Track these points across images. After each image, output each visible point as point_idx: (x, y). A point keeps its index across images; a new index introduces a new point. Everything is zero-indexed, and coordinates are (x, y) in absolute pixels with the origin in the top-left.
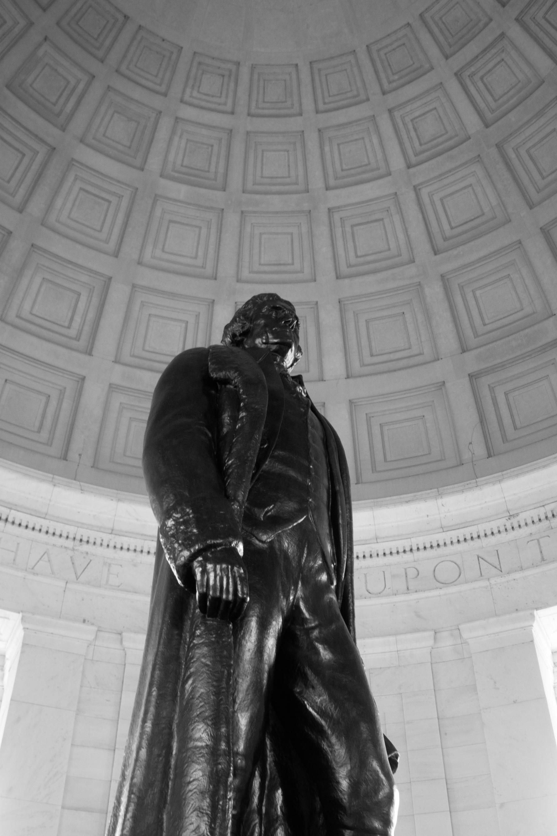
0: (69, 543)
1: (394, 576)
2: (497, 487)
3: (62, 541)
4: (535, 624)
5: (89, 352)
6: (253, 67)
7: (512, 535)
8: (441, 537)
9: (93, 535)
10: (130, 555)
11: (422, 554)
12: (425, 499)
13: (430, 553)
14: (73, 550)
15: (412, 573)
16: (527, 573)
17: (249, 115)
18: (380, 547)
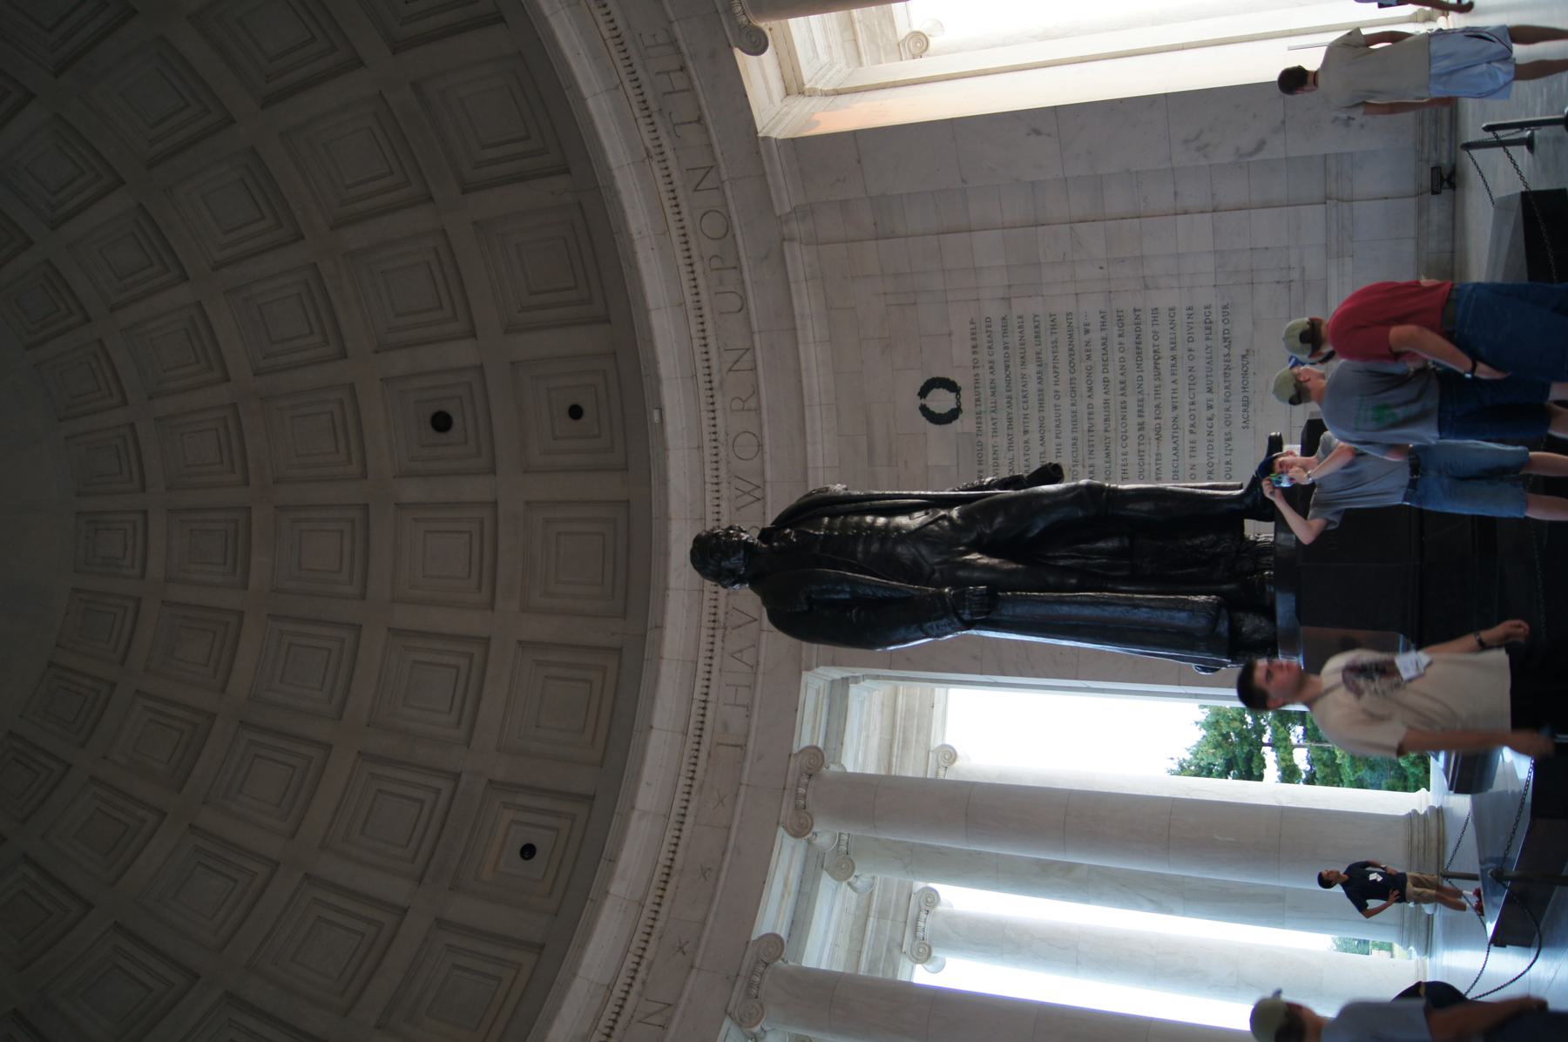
0: (719, 633)
1: (721, 283)
2: (616, 173)
4: (774, 135)
5: (486, 642)
7: (669, 154)
8: (675, 233)
9: (707, 609)
11: (694, 252)
12: (634, 253)
13: (693, 245)
14: (725, 628)
15: (716, 263)
16: (714, 139)
17: (144, 490)
18: (689, 299)
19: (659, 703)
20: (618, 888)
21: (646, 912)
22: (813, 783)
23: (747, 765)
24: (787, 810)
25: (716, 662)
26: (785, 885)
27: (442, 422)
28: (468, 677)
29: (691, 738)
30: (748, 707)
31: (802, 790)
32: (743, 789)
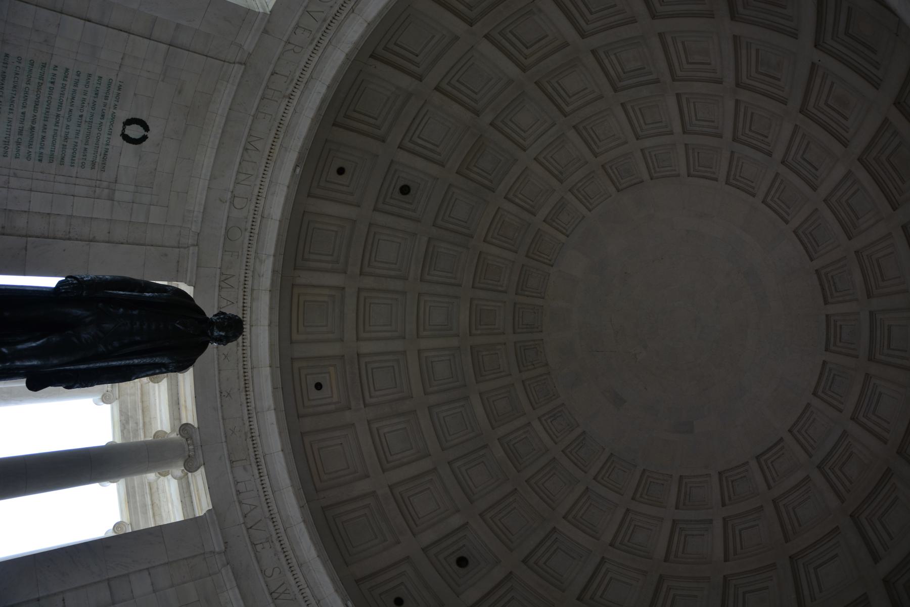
0: (268, 514)
3: (266, 509)
6: (584, 432)
10: (279, 548)
19: (284, 464)
20: (266, 372)
21: (249, 366)
22: (187, 454)
23: (226, 453)
24: (197, 437)
25: (263, 499)
26: (186, 407)
27: (462, 562)
28: (384, 453)
29: (261, 456)
30: (237, 483)
31: (191, 447)
32: (224, 439)
